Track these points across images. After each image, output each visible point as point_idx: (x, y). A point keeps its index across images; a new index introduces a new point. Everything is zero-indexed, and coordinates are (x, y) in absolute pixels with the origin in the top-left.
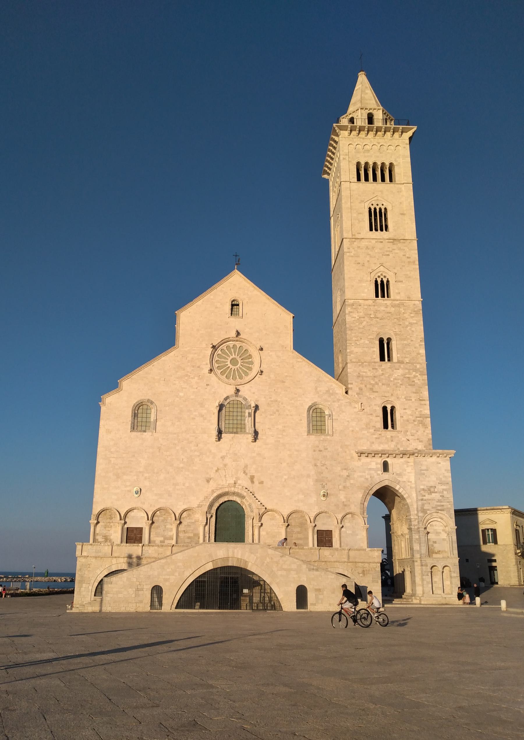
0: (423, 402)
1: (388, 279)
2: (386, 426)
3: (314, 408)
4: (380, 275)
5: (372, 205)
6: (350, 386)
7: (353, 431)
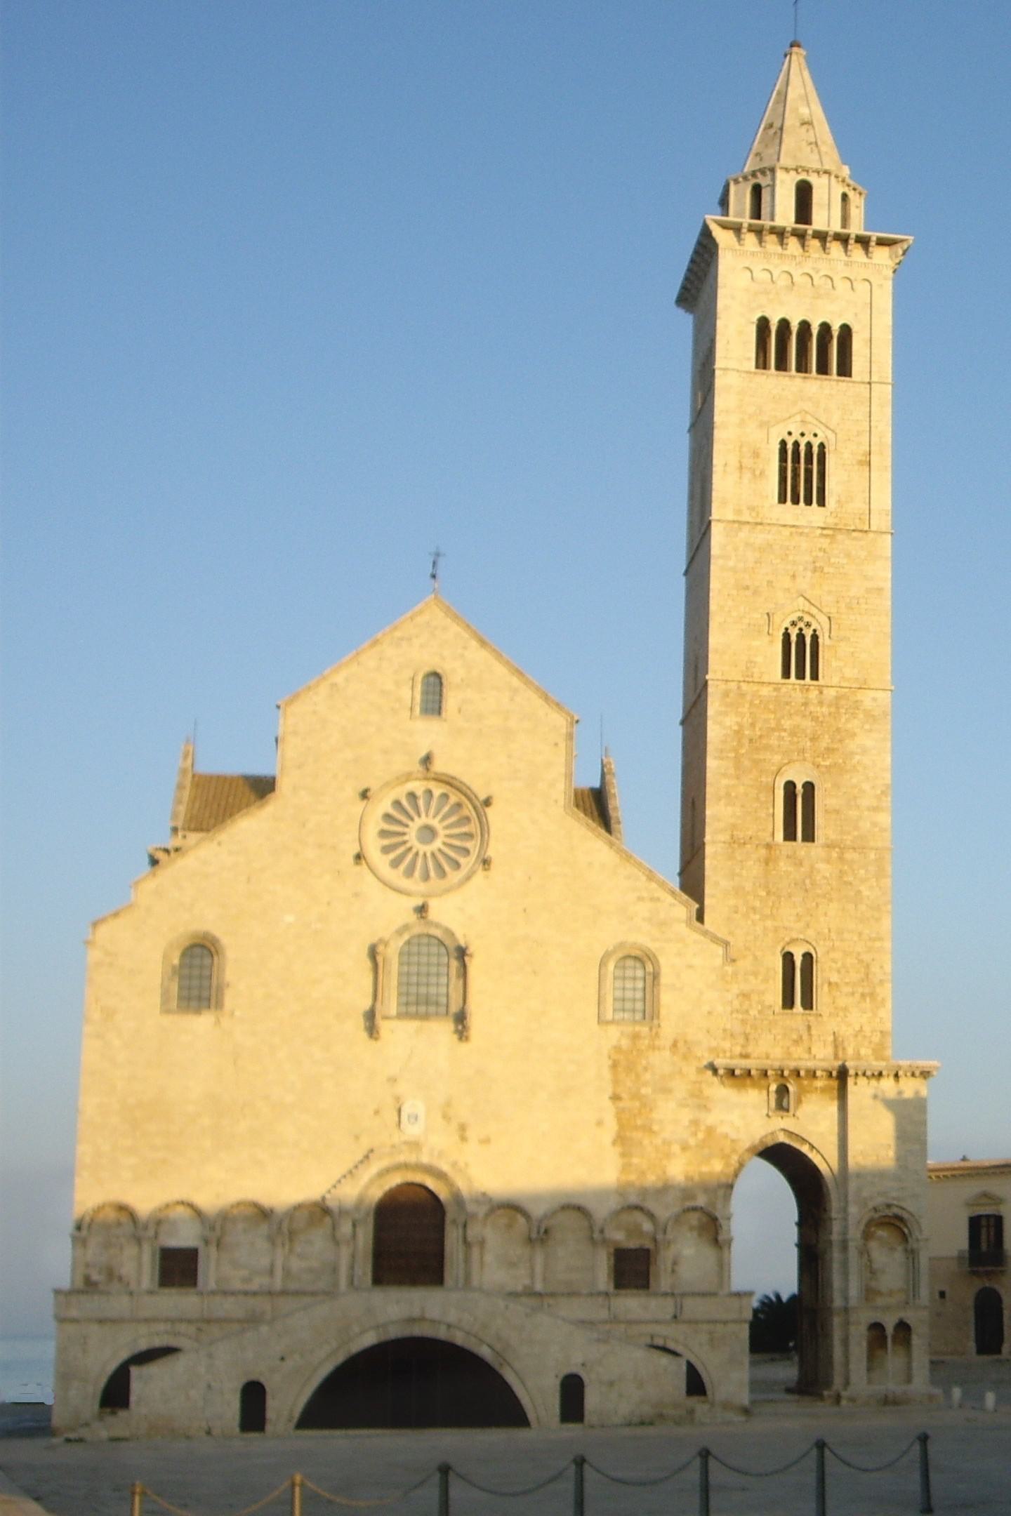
0: (878, 944)
1: (815, 631)
2: (788, 1002)
3: (620, 955)
4: (795, 619)
5: (790, 433)
6: (707, 901)
7: (710, 1013)
